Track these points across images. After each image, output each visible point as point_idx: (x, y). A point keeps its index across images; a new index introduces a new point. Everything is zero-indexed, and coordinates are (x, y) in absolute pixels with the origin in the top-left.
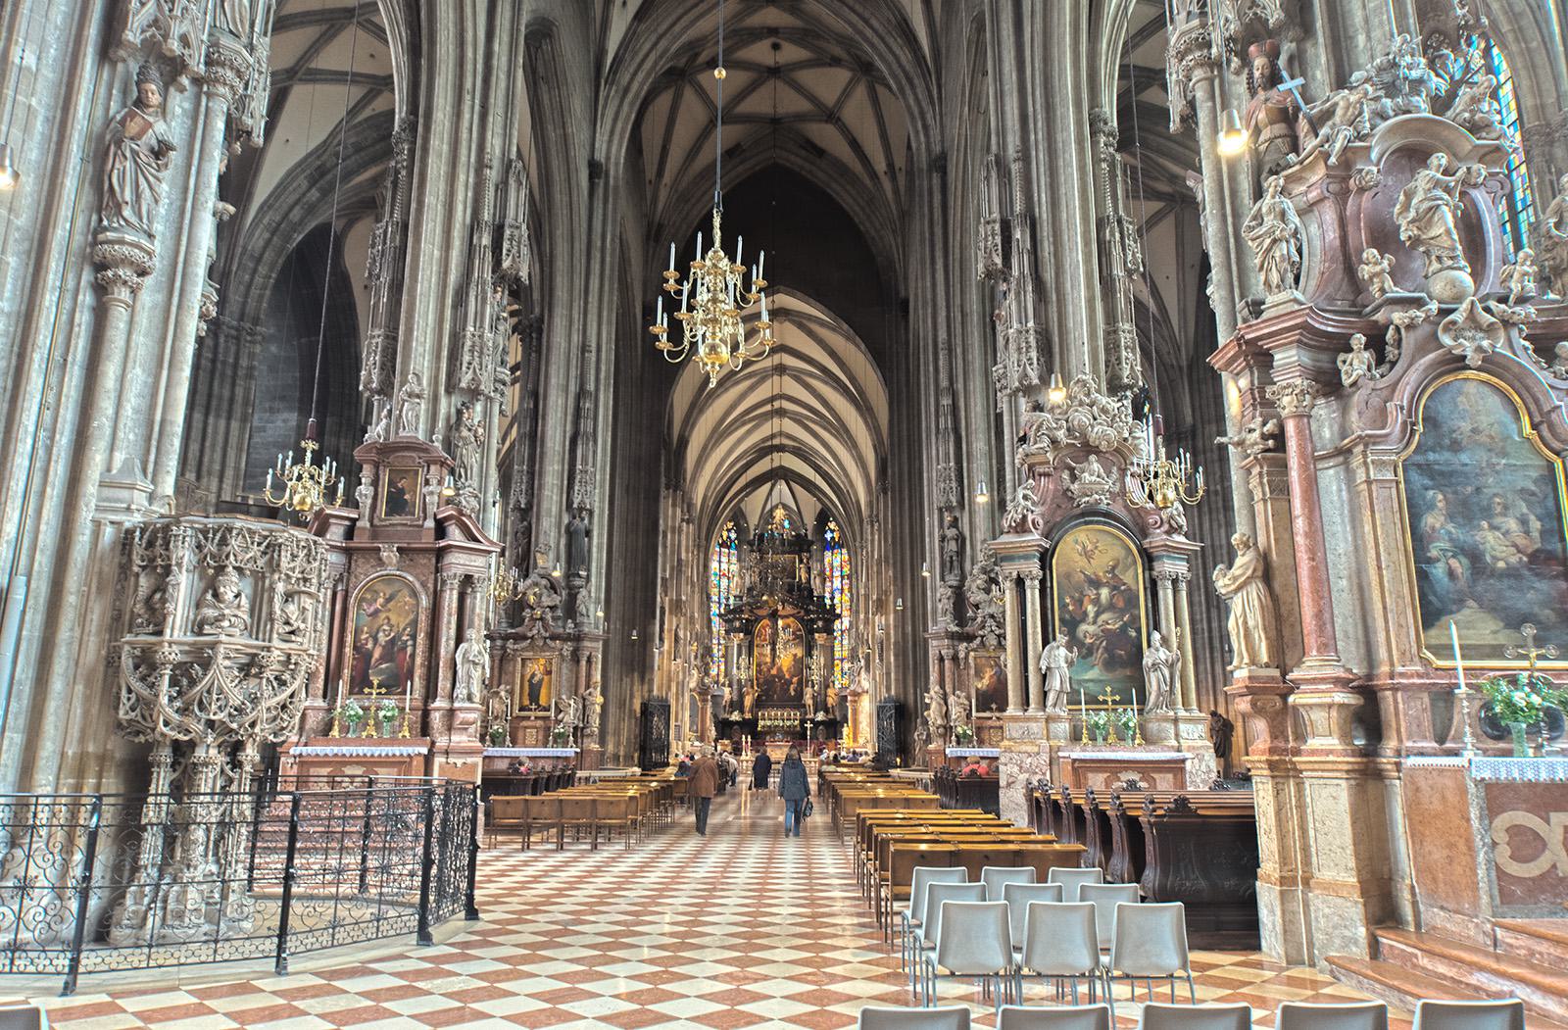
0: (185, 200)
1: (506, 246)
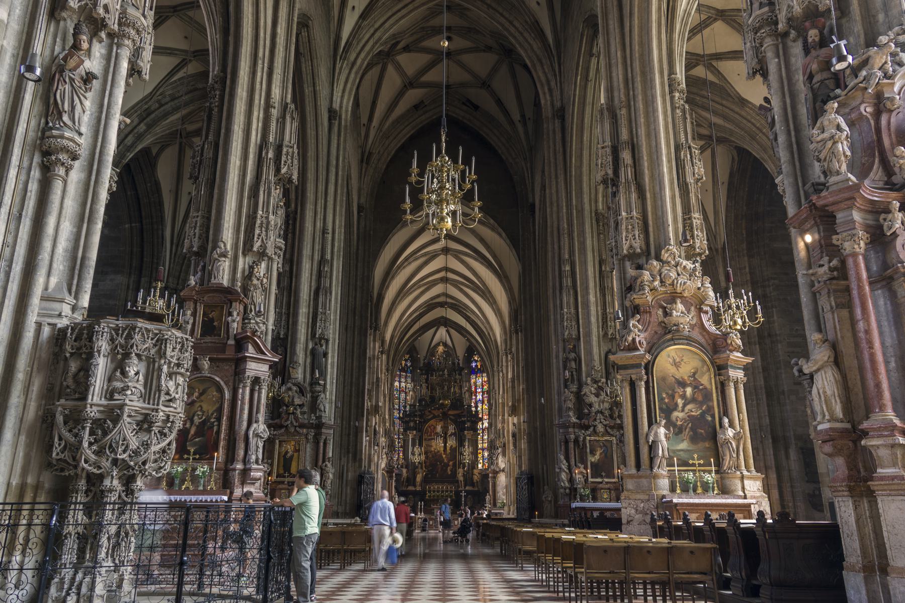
0: (101, 112)
1: (284, 158)
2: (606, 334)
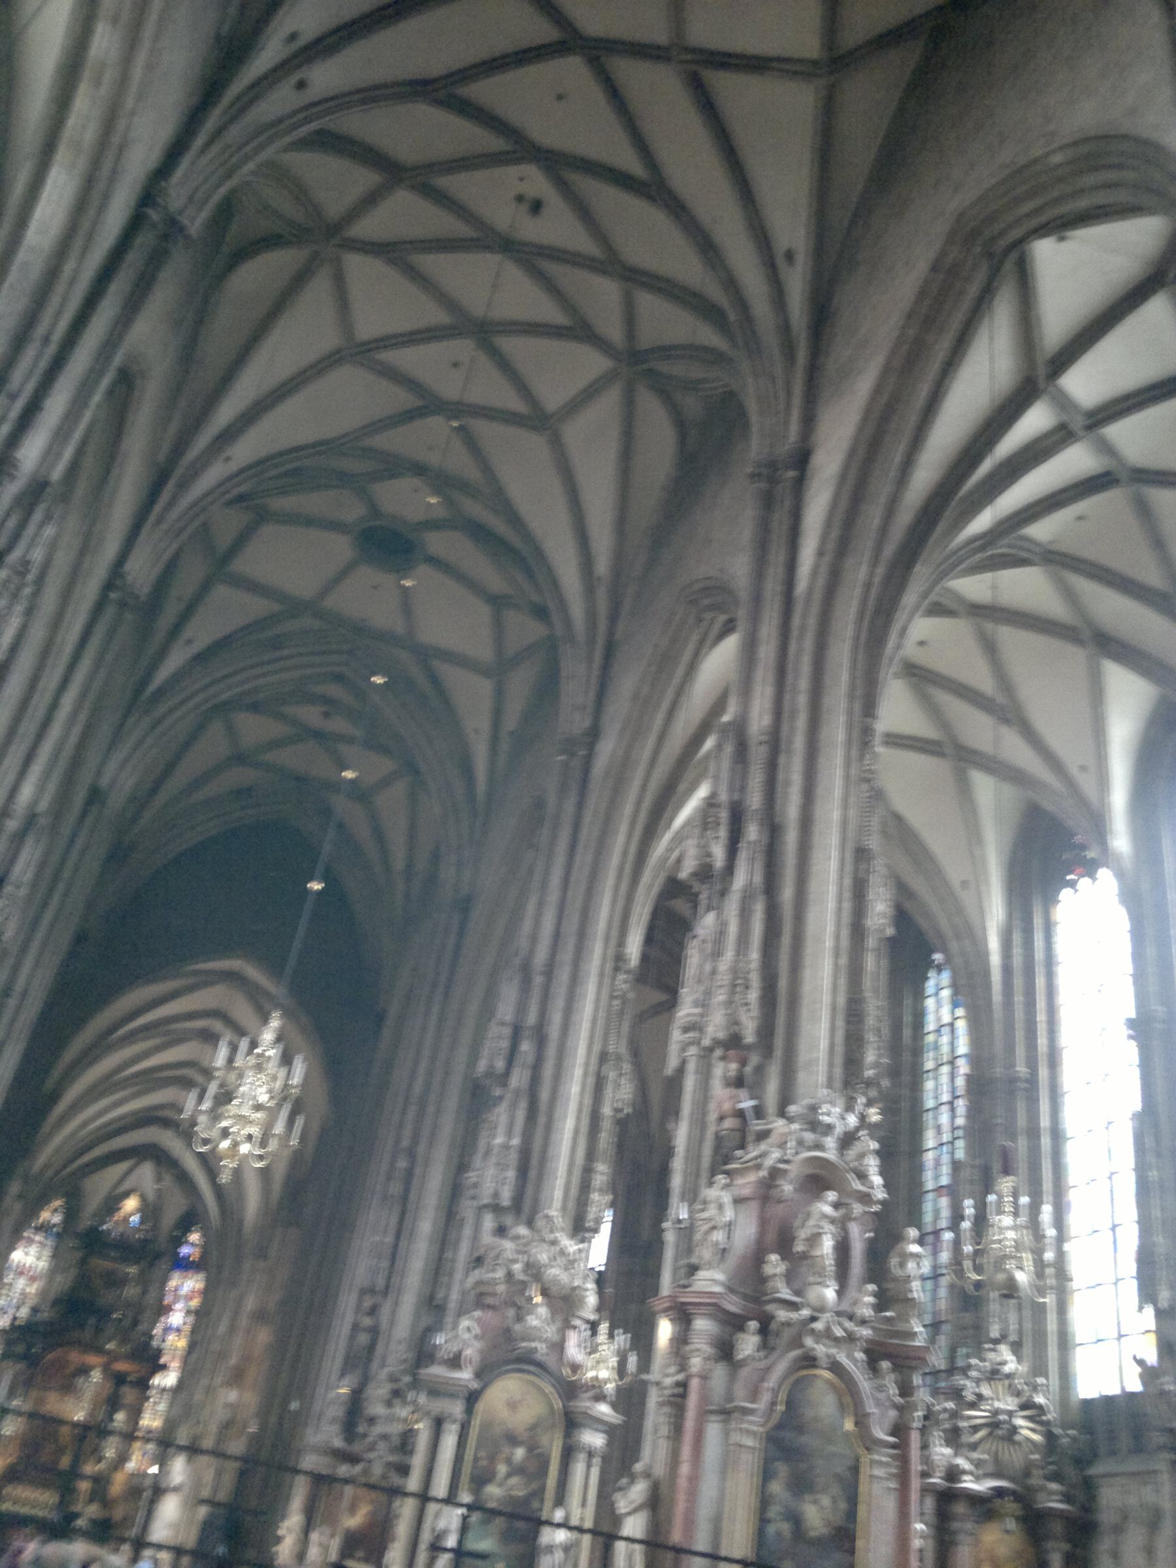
2: (432, 1297)
